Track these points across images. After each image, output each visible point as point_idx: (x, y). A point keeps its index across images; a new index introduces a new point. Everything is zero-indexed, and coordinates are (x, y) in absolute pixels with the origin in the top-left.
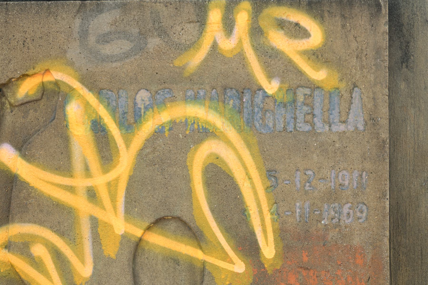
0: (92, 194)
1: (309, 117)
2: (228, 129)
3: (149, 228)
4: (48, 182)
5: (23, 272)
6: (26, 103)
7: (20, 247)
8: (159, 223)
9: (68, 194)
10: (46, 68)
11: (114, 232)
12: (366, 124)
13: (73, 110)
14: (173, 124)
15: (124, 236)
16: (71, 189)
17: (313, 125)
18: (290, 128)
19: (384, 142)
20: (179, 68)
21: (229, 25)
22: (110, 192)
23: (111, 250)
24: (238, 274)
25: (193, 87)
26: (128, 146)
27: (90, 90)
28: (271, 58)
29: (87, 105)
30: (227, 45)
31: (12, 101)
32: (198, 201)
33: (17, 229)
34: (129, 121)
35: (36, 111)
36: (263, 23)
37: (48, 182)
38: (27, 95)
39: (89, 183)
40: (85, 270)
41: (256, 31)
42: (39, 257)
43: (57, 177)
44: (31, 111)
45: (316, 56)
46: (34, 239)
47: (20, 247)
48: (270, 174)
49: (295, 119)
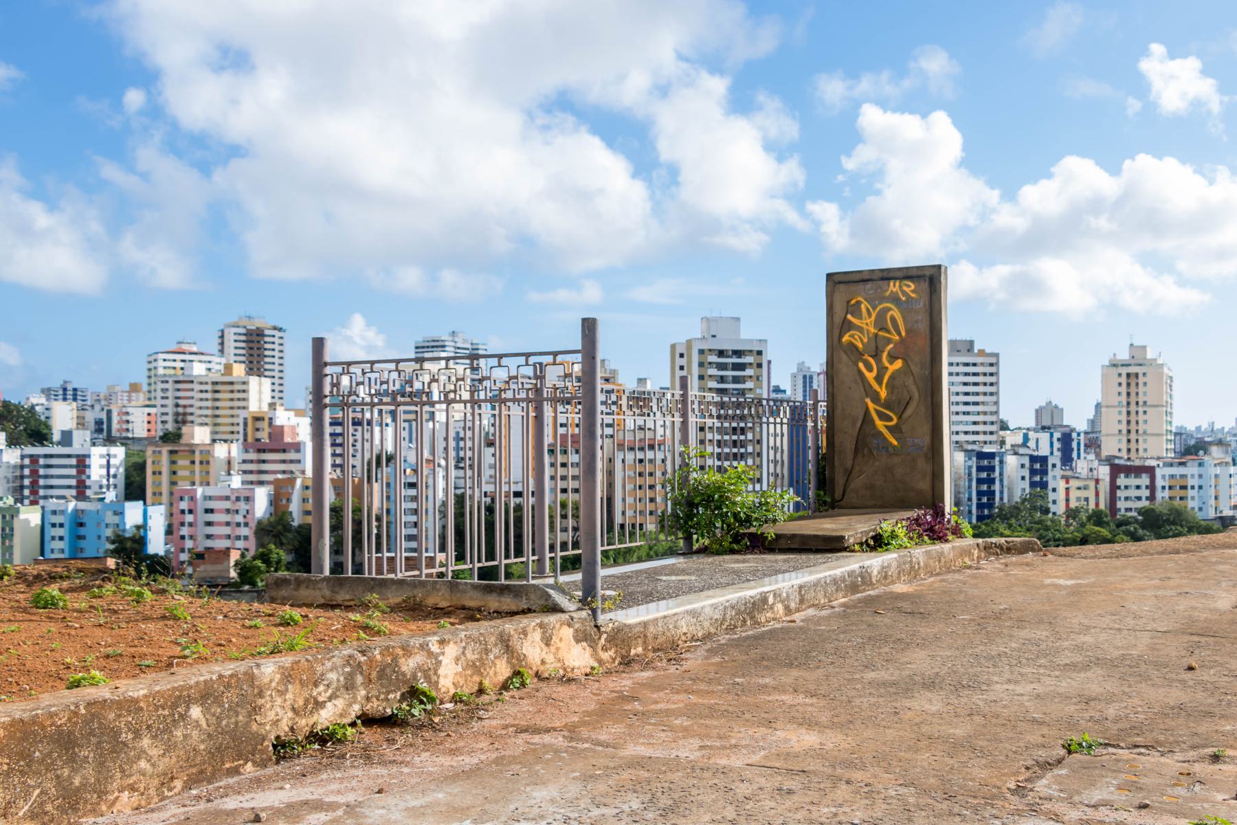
8: (880, 330)
25: (887, 300)
28: (904, 293)
34: (874, 309)
40: (866, 340)
45: (913, 291)
48: (904, 318)
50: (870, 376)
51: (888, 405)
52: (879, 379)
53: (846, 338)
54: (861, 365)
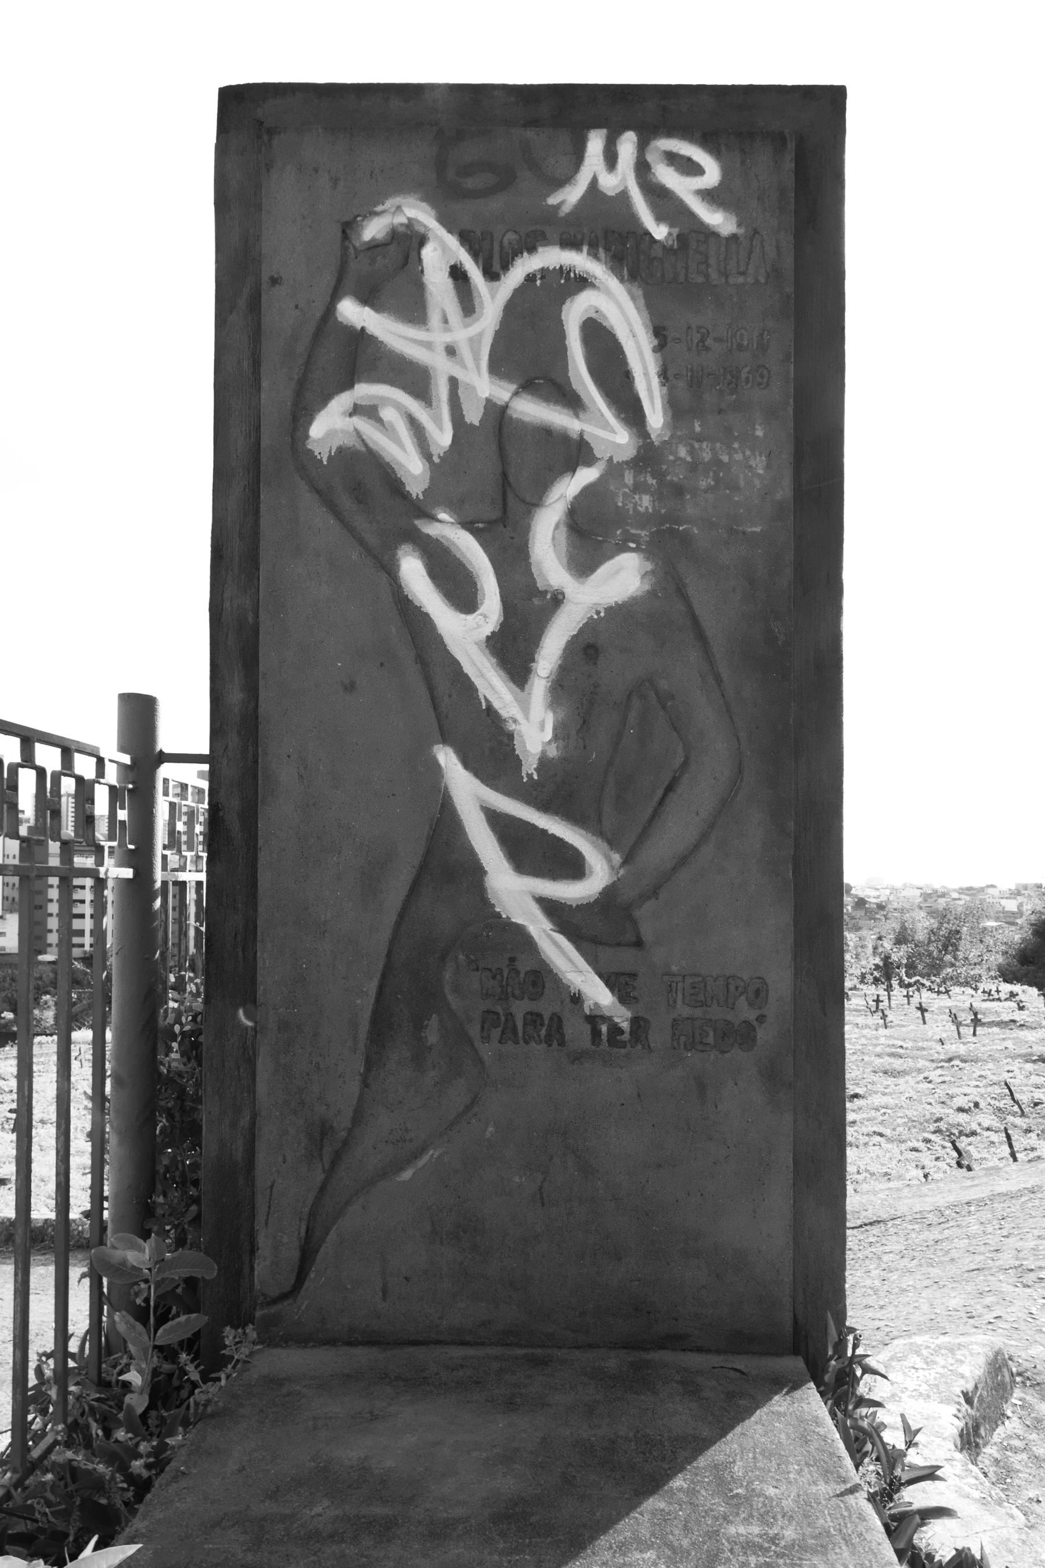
0: (451, 351)
1: (703, 267)
2: (610, 279)
3: (516, 394)
4: (400, 336)
5: (371, 439)
6: (374, 246)
7: (368, 411)
8: (528, 386)
9: (424, 350)
10: (398, 204)
11: (477, 395)
12: (768, 276)
13: (429, 254)
14: (544, 272)
15: (488, 401)
16: (428, 345)
17: (707, 276)
18: (682, 278)
19: (788, 297)
20: (553, 206)
21: (611, 159)
22: (472, 349)
23: (473, 416)
24: (619, 445)
26: (493, 297)
27: (449, 231)
28: (660, 197)
29: (444, 248)
30: (609, 183)
31: (357, 245)
32: (574, 361)
33: (364, 391)
35: (384, 257)
36: (650, 158)
37: (400, 336)
38: (373, 239)
39: (448, 338)
40: (443, 438)
41: (642, 168)
42: (390, 423)
43: (411, 330)
44: (379, 258)
45: (709, 196)
46: (387, 401)
47: (368, 411)
49: (687, 268)
50: (465, 634)
51: (556, 790)
52: (513, 650)
53: (330, 426)
54: (413, 572)
